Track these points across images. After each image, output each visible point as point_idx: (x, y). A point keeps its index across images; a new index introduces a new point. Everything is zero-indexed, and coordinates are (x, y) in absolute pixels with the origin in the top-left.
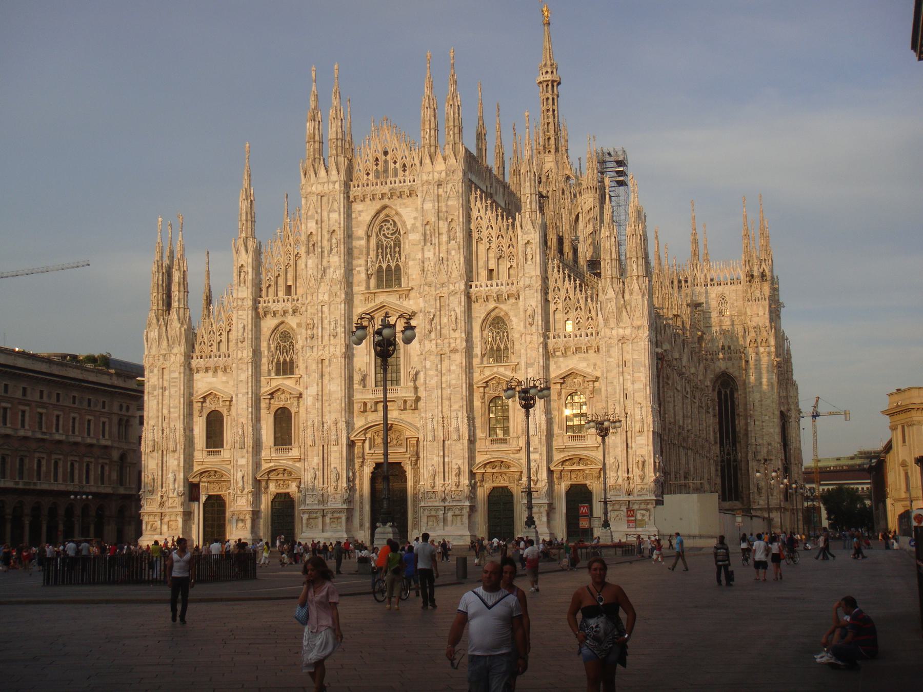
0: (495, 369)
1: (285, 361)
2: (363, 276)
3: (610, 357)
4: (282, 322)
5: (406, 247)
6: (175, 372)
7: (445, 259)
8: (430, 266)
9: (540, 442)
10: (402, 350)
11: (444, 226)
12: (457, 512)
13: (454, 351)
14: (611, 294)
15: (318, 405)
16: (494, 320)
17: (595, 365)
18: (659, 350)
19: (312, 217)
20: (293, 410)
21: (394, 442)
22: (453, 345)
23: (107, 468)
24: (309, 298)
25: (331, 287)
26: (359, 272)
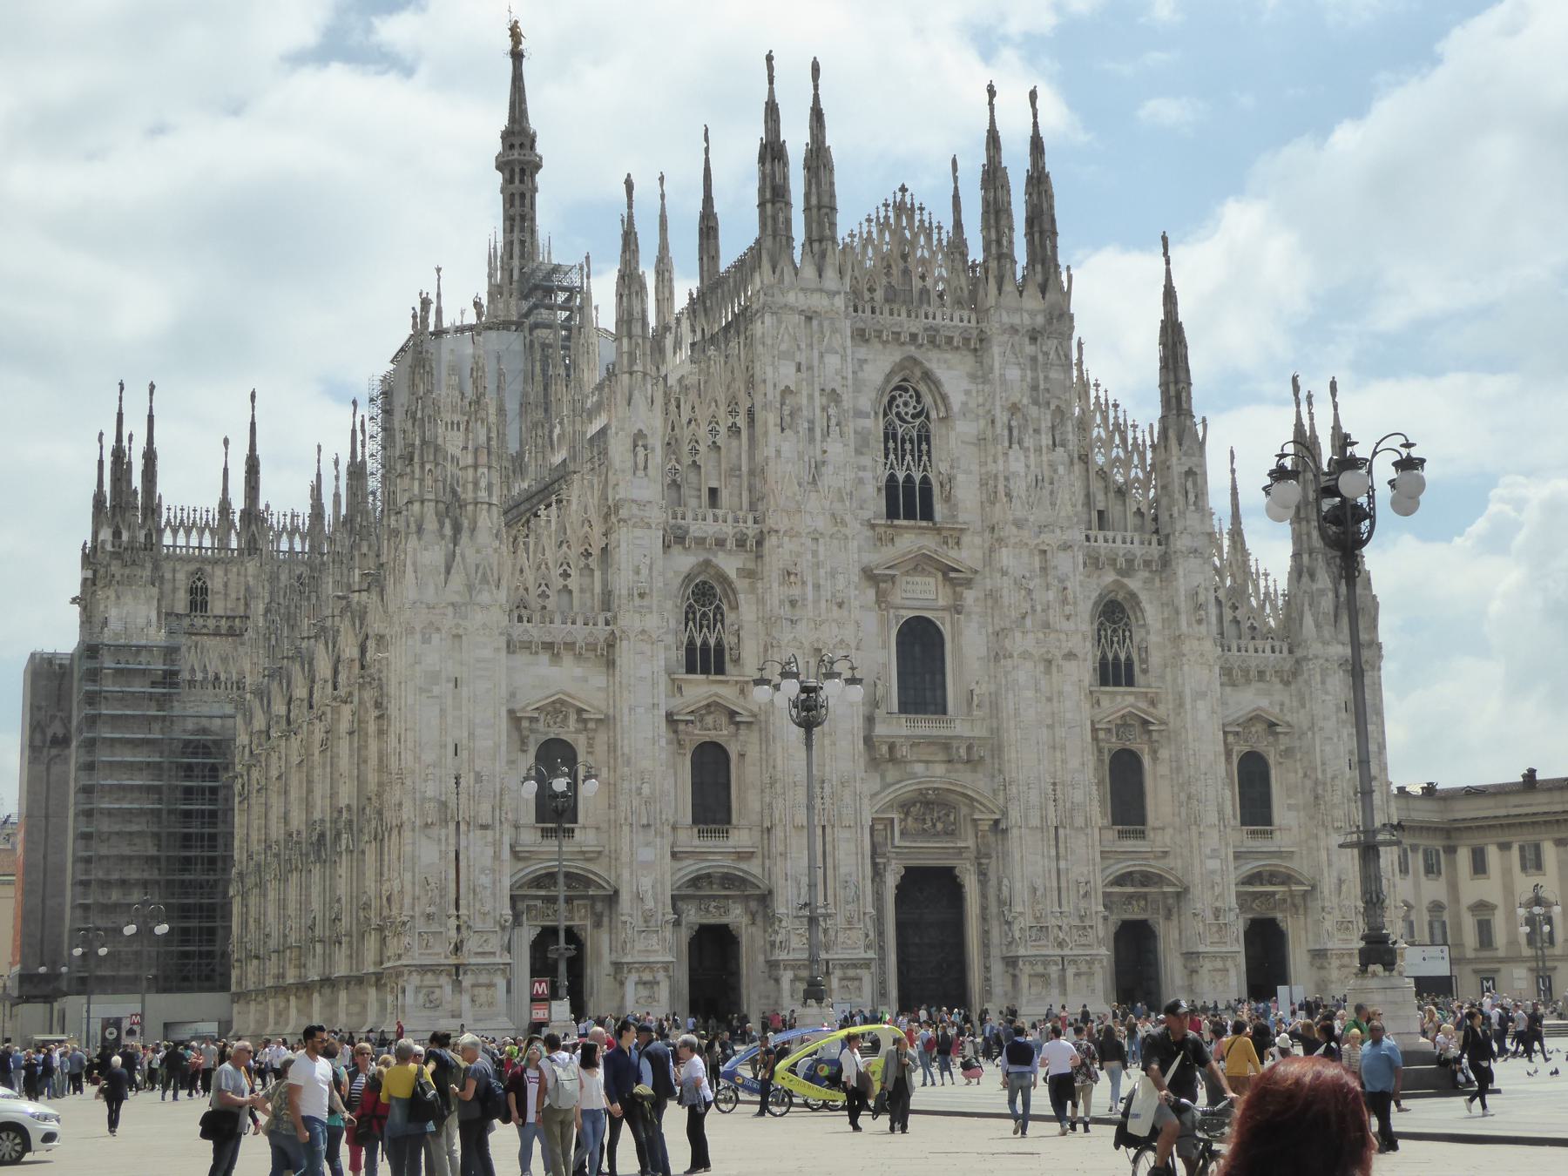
0: (1119, 699)
1: (705, 643)
3: (1327, 693)
4: (707, 563)
12: (1084, 968)
13: (1070, 656)
17: (1282, 704)
20: (733, 751)
21: (939, 826)
22: (1067, 646)
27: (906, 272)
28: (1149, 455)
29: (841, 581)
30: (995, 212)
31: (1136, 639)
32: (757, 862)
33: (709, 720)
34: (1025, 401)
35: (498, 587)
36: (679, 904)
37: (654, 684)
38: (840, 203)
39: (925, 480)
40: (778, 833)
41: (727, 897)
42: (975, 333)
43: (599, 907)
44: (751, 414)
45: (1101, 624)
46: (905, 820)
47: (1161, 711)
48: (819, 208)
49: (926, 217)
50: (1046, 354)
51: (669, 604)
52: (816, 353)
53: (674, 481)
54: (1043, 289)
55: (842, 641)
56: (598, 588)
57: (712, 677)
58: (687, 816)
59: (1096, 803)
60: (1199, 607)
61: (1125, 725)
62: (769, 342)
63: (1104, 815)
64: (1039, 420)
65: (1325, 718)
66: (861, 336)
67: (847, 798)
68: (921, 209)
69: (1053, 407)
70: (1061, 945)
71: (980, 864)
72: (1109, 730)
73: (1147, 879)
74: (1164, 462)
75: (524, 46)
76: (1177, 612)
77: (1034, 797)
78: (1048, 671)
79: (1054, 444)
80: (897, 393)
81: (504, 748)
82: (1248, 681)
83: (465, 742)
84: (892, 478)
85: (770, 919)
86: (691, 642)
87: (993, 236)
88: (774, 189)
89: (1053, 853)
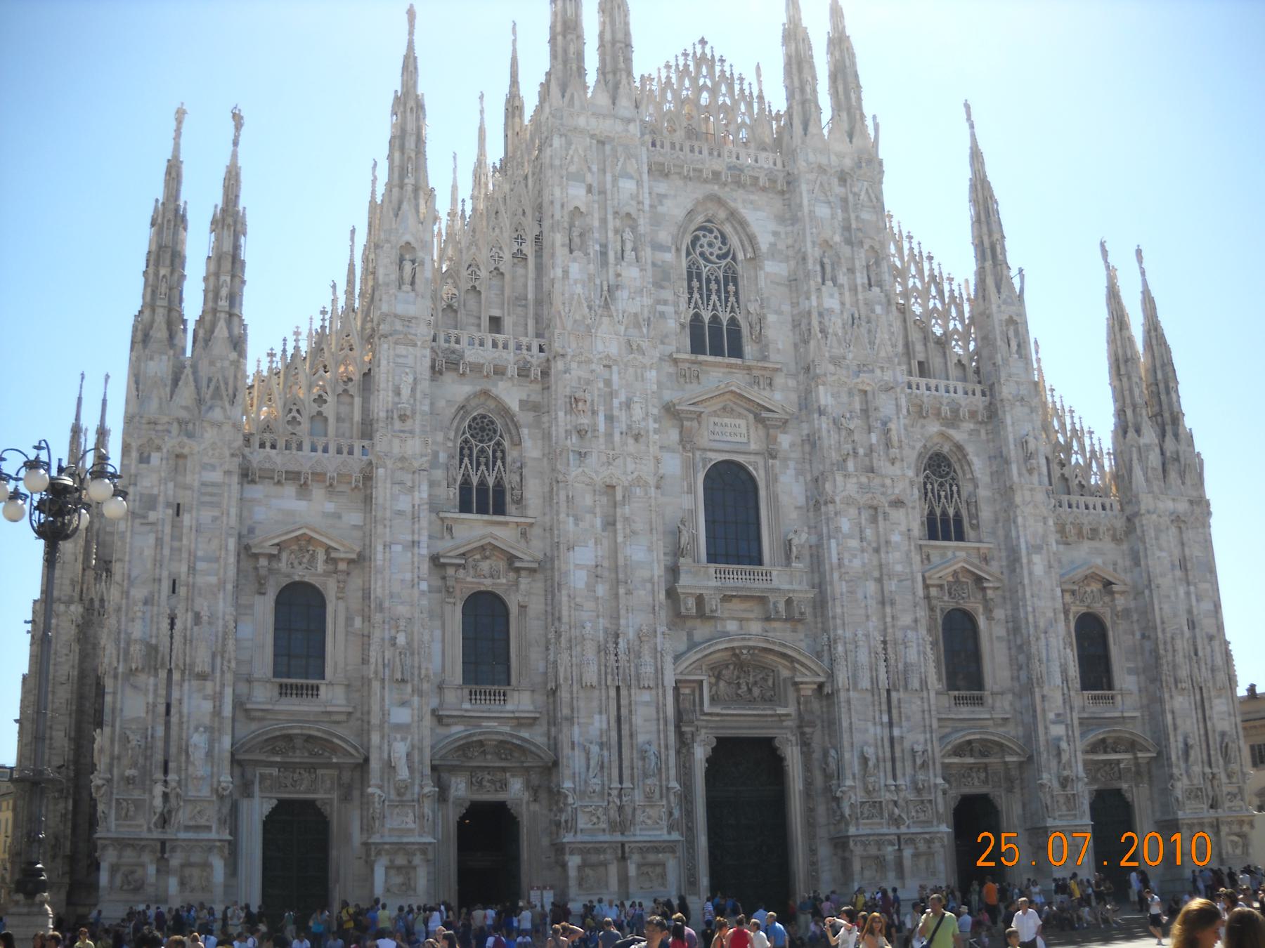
0: (950, 554)
1: (482, 483)
2: (672, 324)
3: (1161, 549)
6: (213, 468)
7: (863, 317)
10: (762, 493)
13: (898, 503)
14: (1149, 436)
15: (601, 590)
16: (930, 458)
17: (1115, 564)
19: (578, 177)
21: (756, 691)
24: (574, 345)
25: (626, 329)
26: (662, 315)
28: (967, 308)
29: (638, 412)
30: (797, 65)
31: (964, 494)
32: (541, 729)
33: (485, 566)
34: (837, 238)
35: (232, 403)
37: (415, 518)
38: (634, 44)
39: (733, 321)
40: (564, 694)
41: (504, 769)
42: (781, 175)
43: (346, 777)
44: (538, 239)
45: (927, 477)
46: (717, 684)
47: (995, 567)
48: (614, 42)
49: (727, 68)
50: (856, 195)
51: (440, 437)
52: (609, 178)
53: (450, 306)
54: (851, 136)
55: (639, 477)
56: (357, 416)
57: (485, 517)
58: (456, 673)
59: (932, 665)
60: (1029, 457)
61: (957, 581)
62: (557, 162)
63: (939, 680)
64: (853, 259)
65: (1163, 575)
66: (659, 171)
67: (647, 657)
68: (722, 61)
69: (866, 247)
70: (897, 821)
71: (803, 734)
72: (941, 587)
73: (985, 748)
74: (982, 314)
76: (1007, 462)
77: (863, 657)
78: (874, 520)
79: (870, 285)
80: (700, 233)
81: (230, 587)
83: (183, 577)
85: (556, 796)
87: (796, 83)
88: (565, 23)
89: (885, 718)
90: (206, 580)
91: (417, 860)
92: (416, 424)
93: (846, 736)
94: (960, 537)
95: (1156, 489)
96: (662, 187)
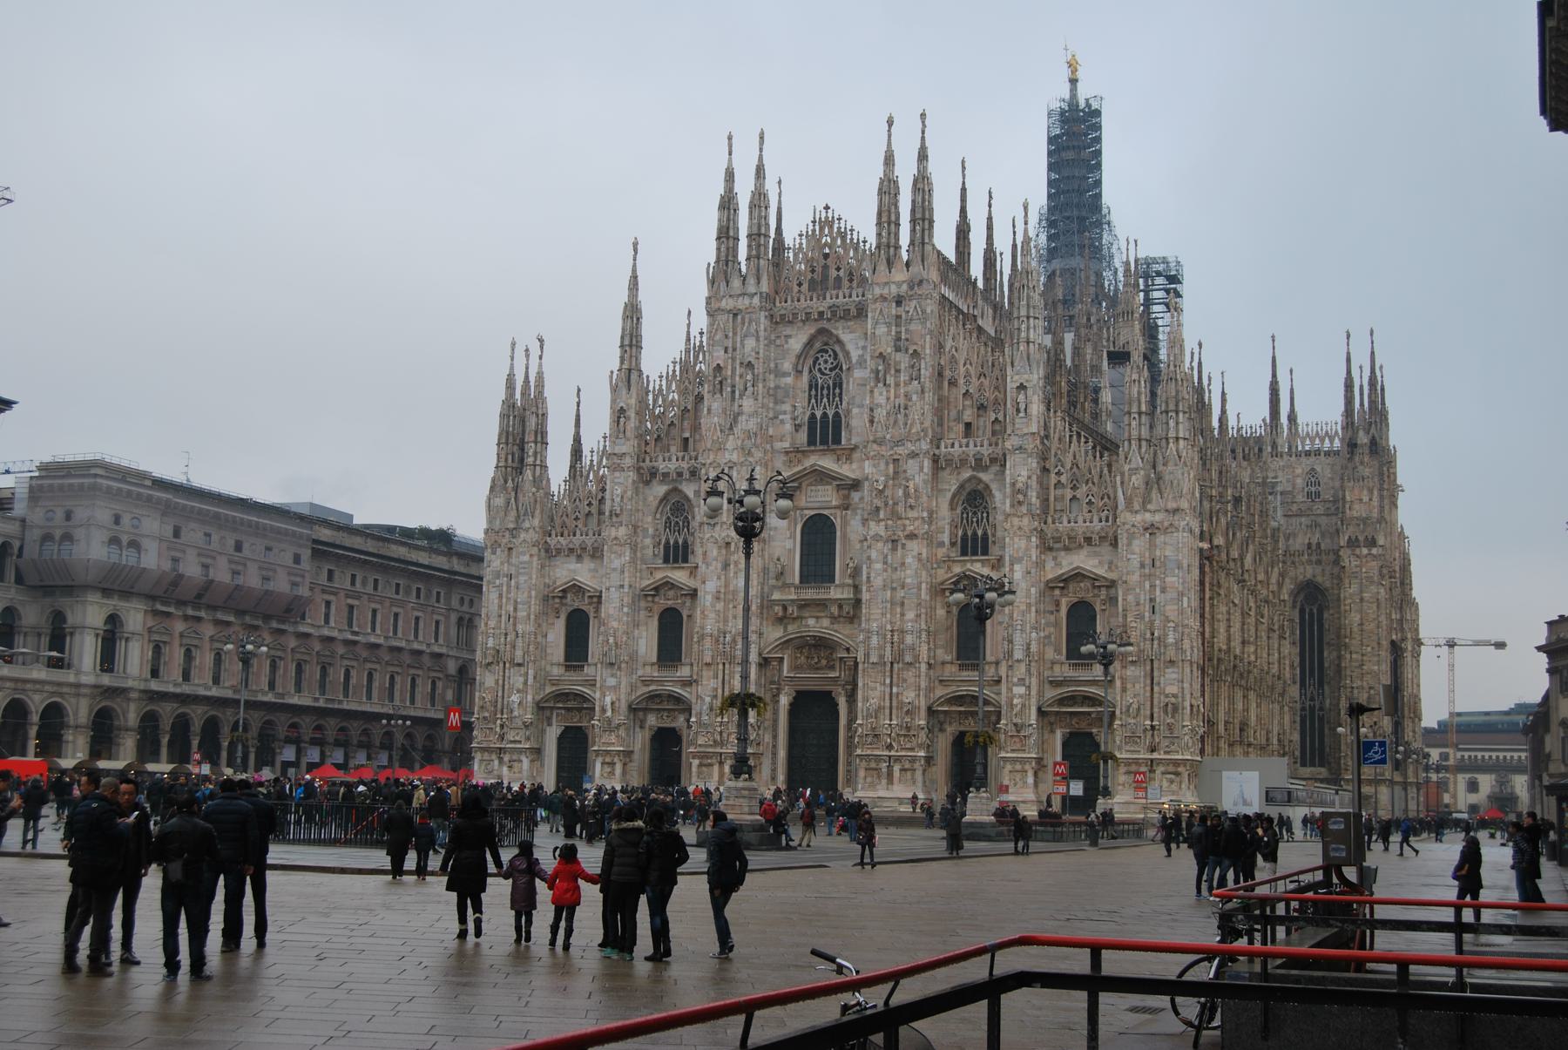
0: (969, 566)
1: (676, 542)
2: (788, 427)
5: (851, 387)
8: (881, 414)
9: (1029, 671)
11: (903, 360)
12: (907, 766)
13: (912, 536)
14: (1136, 461)
17: (1111, 563)
18: (1206, 546)
21: (824, 662)
23: (440, 684)
26: (782, 422)
27: (825, 267)
36: (641, 714)
39: (837, 415)
51: (650, 519)
70: (890, 747)
75: (1080, 75)
78: (894, 549)
82: (1080, 546)
84: (813, 416)
86: (667, 542)
90: (522, 614)
91: (616, 760)
92: (624, 518)
93: (860, 693)
94: (985, 552)
95: (1137, 506)
96: (788, 331)
